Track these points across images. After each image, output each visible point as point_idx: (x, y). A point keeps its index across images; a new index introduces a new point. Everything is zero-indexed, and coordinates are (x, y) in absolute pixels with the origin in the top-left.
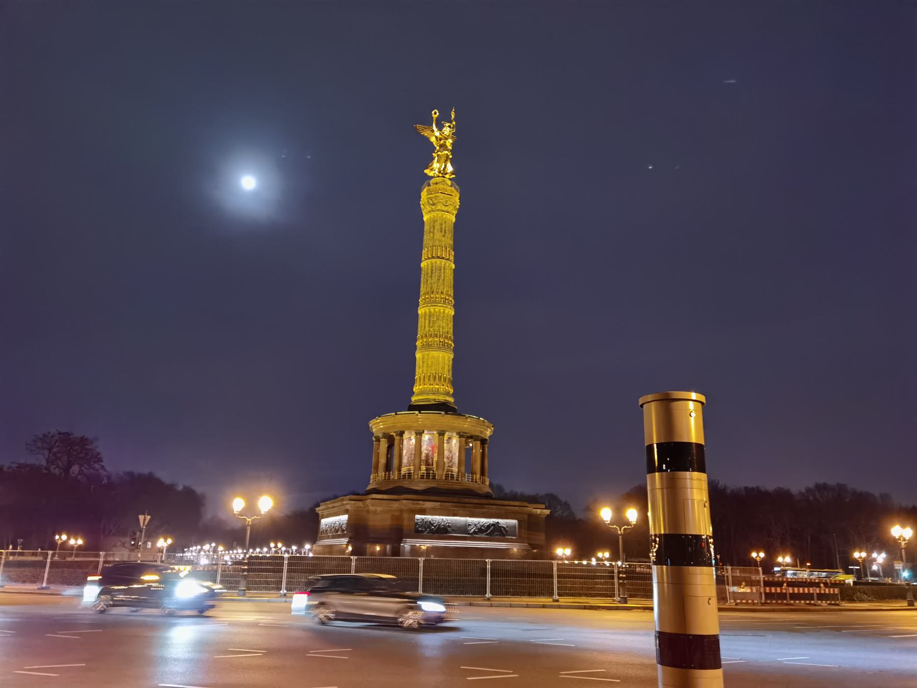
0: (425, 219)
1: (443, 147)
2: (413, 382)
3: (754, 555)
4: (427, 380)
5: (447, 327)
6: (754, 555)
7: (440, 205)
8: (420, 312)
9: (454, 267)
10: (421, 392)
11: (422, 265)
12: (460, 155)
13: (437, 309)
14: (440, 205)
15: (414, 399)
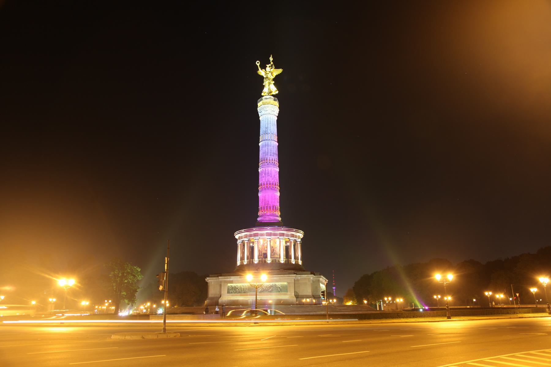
0: (260, 119)
1: (267, 78)
2: (258, 210)
3: (435, 297)
4: (266, 208)
5: (275, 178)
6: (435, 297)
7: (268, 111)
8: (259, 170)
9: (277, 144)
10: (263, 215)
11: (260, 144)
12: (277, 80)
13: (270, 169)
14: (268, 111)
15: (258, 219)
